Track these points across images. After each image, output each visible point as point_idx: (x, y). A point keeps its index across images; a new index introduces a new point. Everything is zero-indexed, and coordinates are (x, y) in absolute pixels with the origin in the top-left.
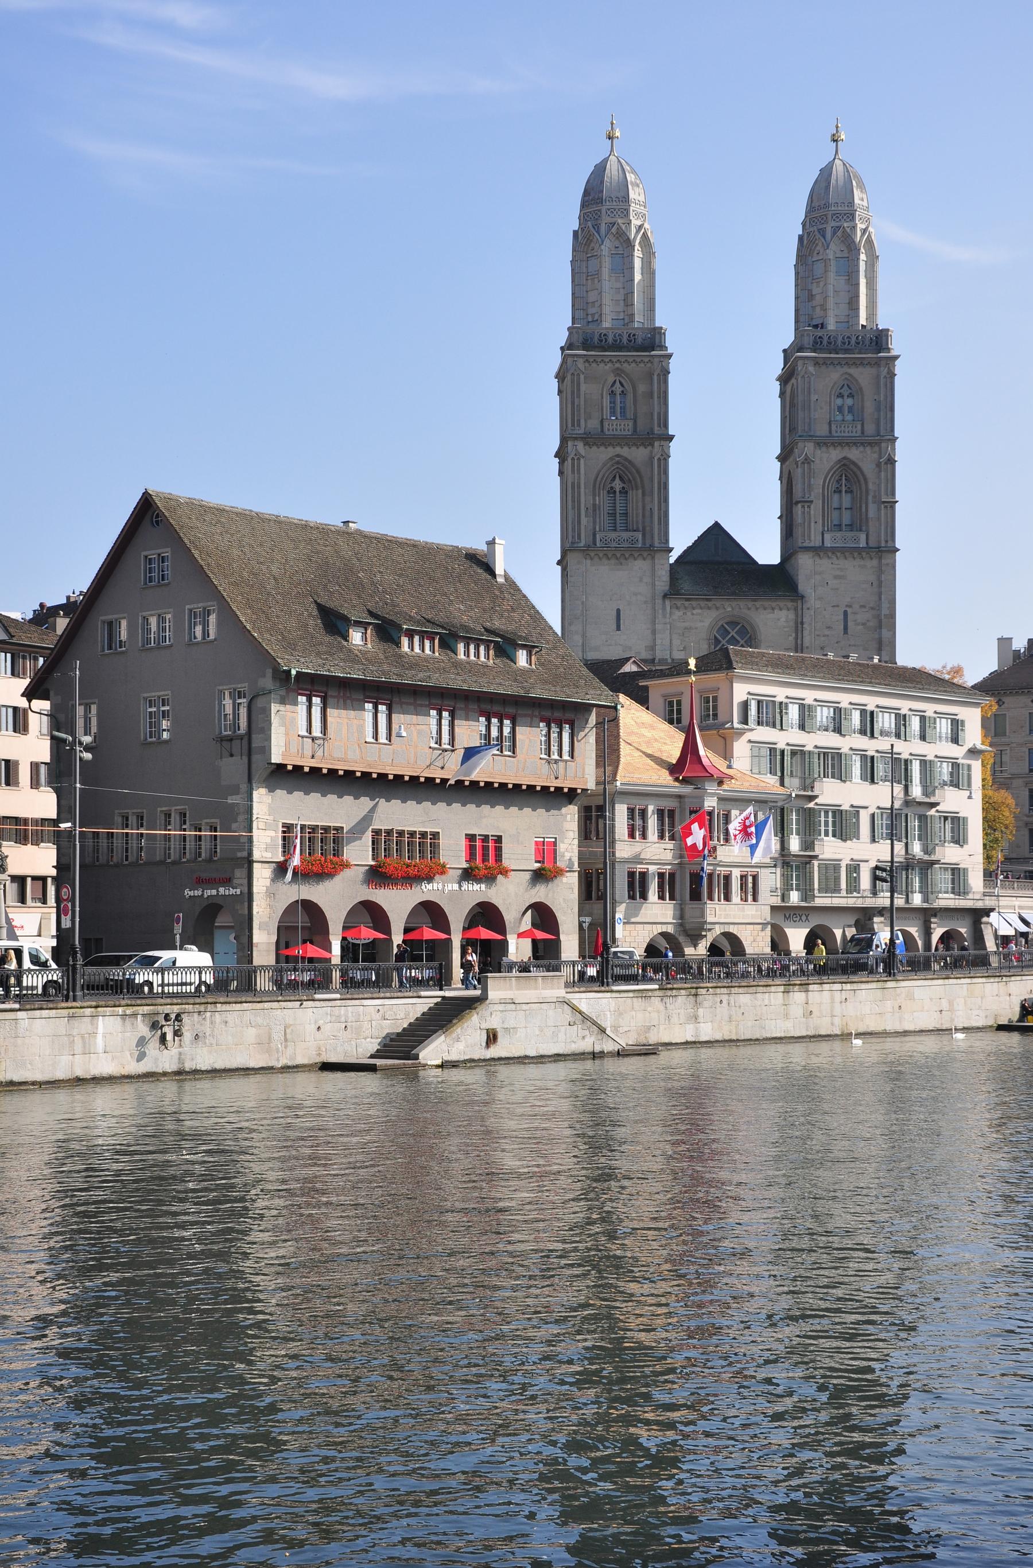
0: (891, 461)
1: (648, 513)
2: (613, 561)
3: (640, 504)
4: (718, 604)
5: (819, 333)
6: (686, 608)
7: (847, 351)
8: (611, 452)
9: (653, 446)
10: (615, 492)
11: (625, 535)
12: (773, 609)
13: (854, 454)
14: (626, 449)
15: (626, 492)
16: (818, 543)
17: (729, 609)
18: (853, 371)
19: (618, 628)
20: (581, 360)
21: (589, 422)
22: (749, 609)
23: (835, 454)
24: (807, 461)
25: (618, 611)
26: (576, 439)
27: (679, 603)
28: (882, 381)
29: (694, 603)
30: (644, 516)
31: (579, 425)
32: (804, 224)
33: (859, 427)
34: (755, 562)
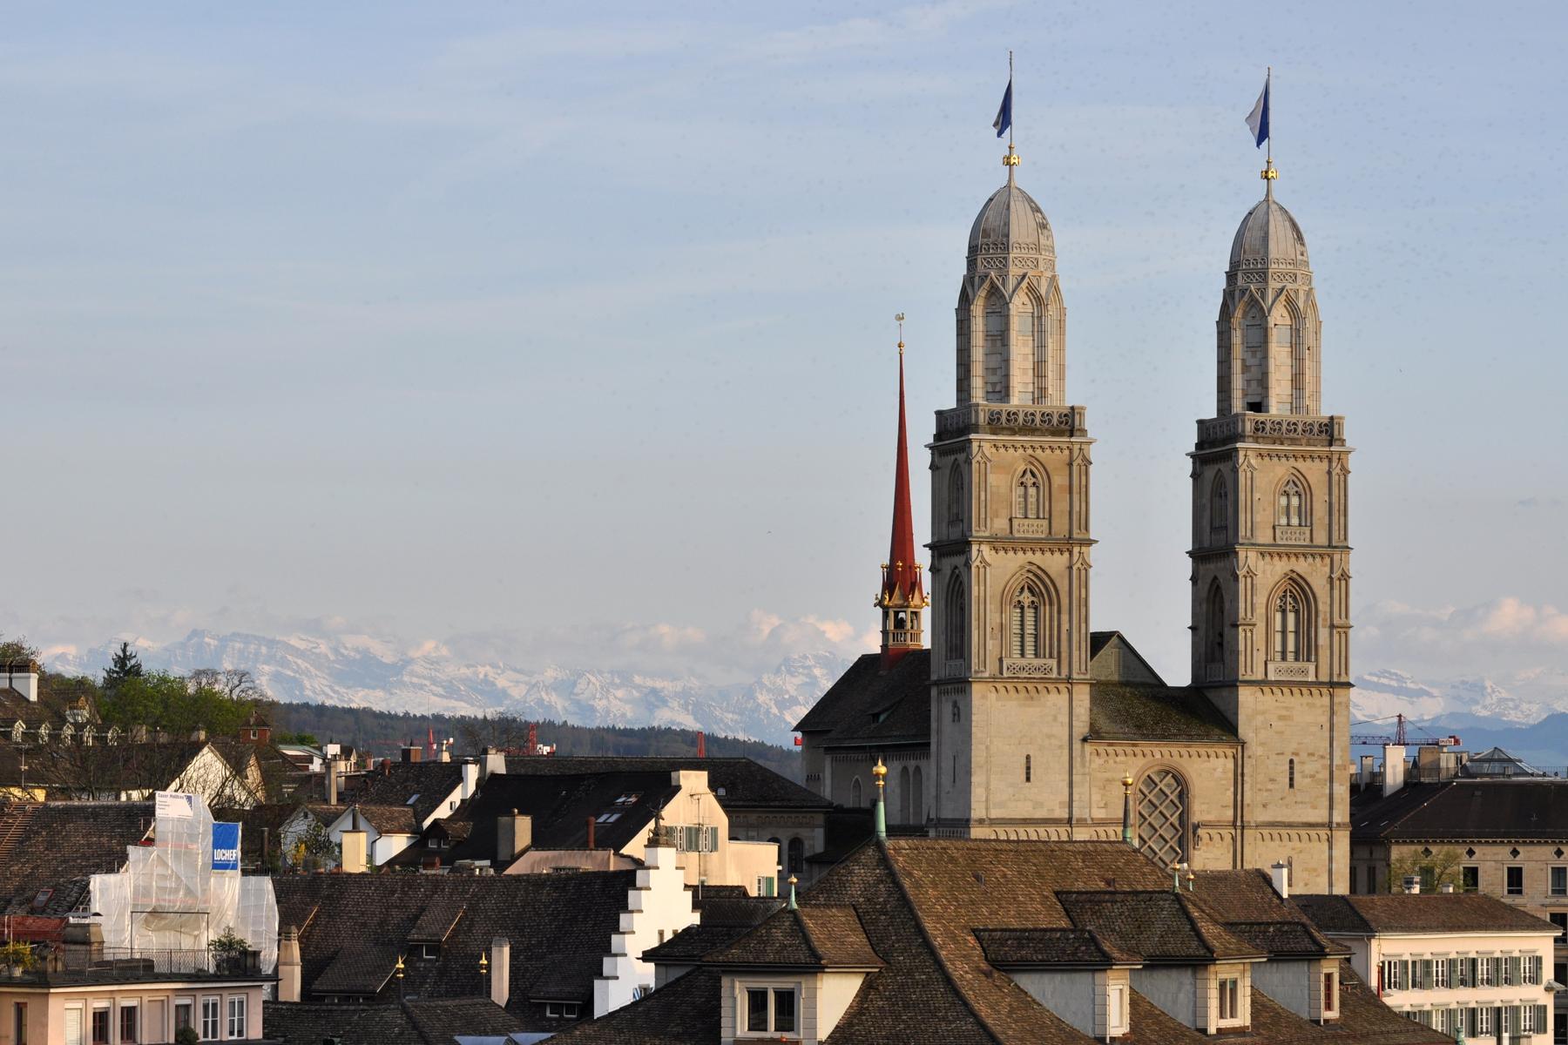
0: (1345, 577)
2: (1023, 693)
4: (1147, 750)
5: (1261, 417)
7: (1293, 441)
8: (1021, 558)
10: (1022, 608)
11: (1037, 662)
13: (1302, 566)
14: (1038, 554)
16: (1259, 676)
18: (1300, 464)
19: (1028, 779)
23: (1280, 567)
24: (1251, 574)
25: (1028, 757)
26: (980, 543)
27: (1101, 749)
28: (1335, 478)
29: (1119, 749)
32: (1231, 276)
34: (1162, 684)
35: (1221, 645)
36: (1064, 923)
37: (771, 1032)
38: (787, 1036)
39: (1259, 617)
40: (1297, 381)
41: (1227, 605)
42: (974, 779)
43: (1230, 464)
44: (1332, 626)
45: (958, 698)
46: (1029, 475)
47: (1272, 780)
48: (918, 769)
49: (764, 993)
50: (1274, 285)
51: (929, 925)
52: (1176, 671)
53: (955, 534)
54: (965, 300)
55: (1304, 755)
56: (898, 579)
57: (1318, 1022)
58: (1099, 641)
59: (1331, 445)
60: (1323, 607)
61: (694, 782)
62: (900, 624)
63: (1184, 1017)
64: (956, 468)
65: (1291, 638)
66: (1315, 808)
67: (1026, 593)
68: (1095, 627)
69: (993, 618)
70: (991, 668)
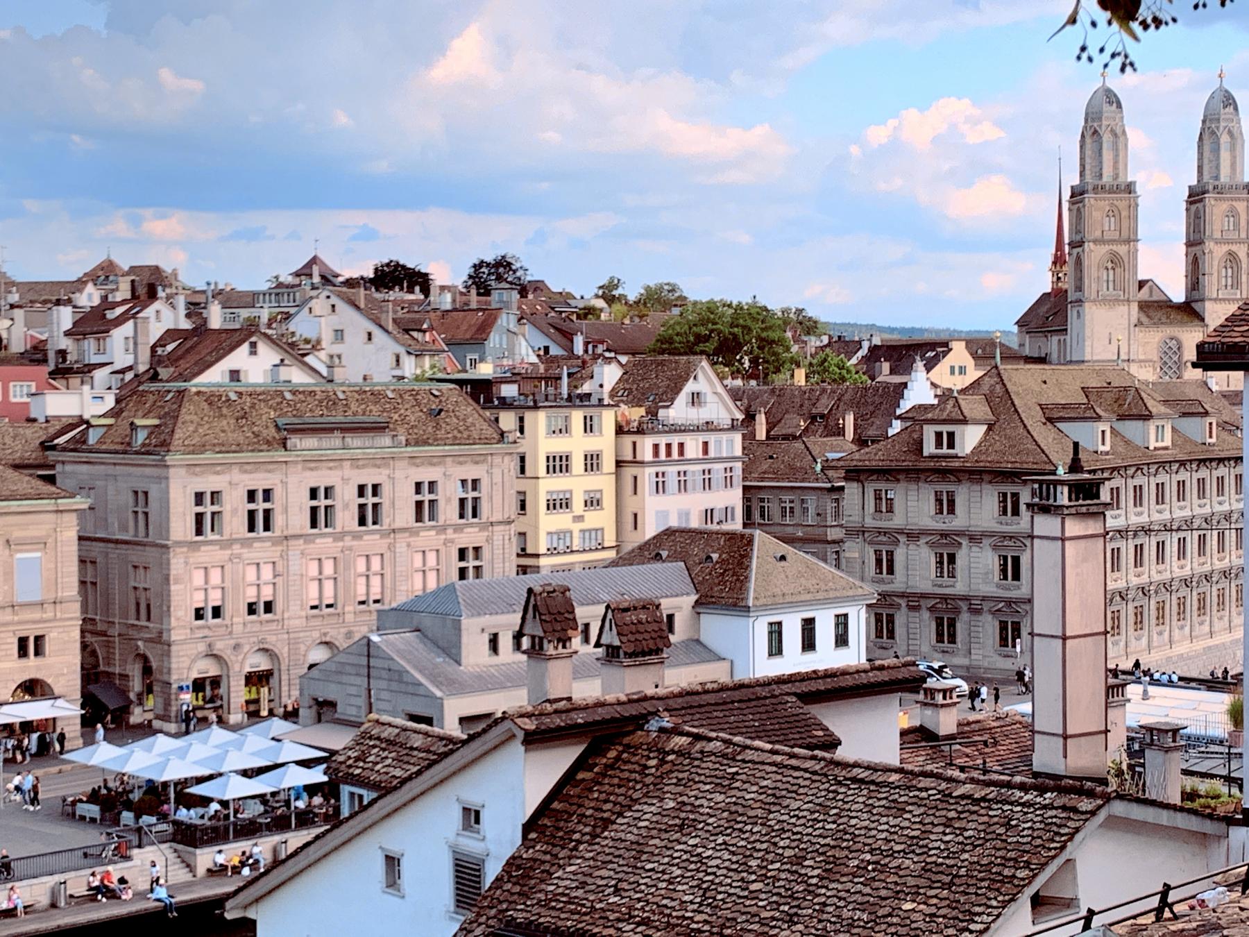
8: (1107, 248)
13: (1234, 248)
16: (1215, 296)
23: (1225, 248)
24: (1211, 252)
32: (1204, 122)
36: (1085, 401)
37: (945, 451)
38: (951, 451)
40: (1233, 165)
50: (1223, 124)
52: (1178, 294)
53: (1078, 238)
54: (1083, 136)
56: (1058, 261)
58: (1142, 284)
61: (959, 348)
63: (1139, 442)
64: (1079, 209)
65: (1229, 280)
68: (1141, 277)
69: (1094, 274)
70: (1094, 295)
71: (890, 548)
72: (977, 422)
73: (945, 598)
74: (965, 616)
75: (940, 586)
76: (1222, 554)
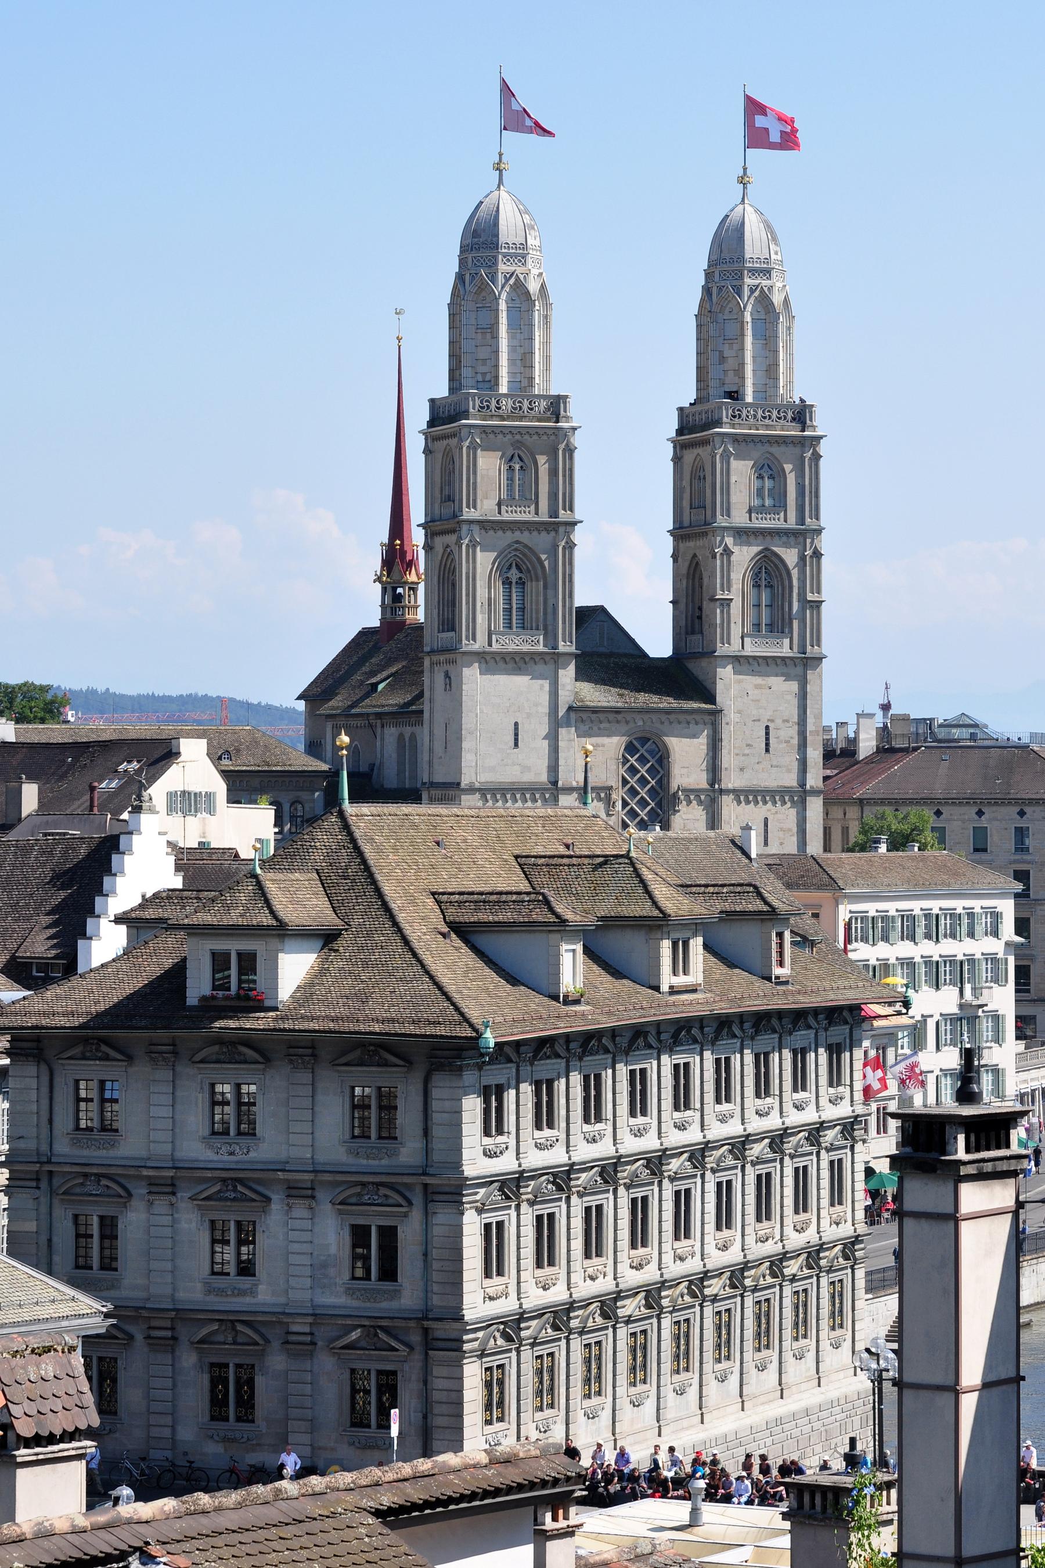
0: (817, 555)
1: (550, 610)
3: (541, 599)
6: (592, 721)
9: (557, 531)
10: (510, 583)
12: (688, 723)
14: (526, 533)
15: (524, 583)
17: (640, 723)
19: (516, 745)
20: (478, 431)
21: (485, 502)
22: (662, 723)
24: (728, 552)
25: (516, 724)
30: (545, 613)
31: (475, 507)
33: (782, 514)
34: (645, 655)
35: (700, 618)
36: (524, 886)
39: (735, 594)
41: (706, 581)
42: (464, 745)
43: (709, 448)
44: (804, 601)
45: (451, 668)
46: (516, 458)
47: (748, 745)
48: (413, 736)
49: (227, 955)
51: (387, 889)
52: (656, 640)
53: (447, 511)
55: (779, 722)
57: (769, 979)
59: (803, 431)
60: (795, 582)
62: (397, 598)
66: (789, 771)
67: (514, 570)
68: (583, 598)
71: (108, 1211)
72: (305, 935)
73: (230, 1322)
74: (277, 1361)
75: (220, 1292)
76: (803, 1216)
